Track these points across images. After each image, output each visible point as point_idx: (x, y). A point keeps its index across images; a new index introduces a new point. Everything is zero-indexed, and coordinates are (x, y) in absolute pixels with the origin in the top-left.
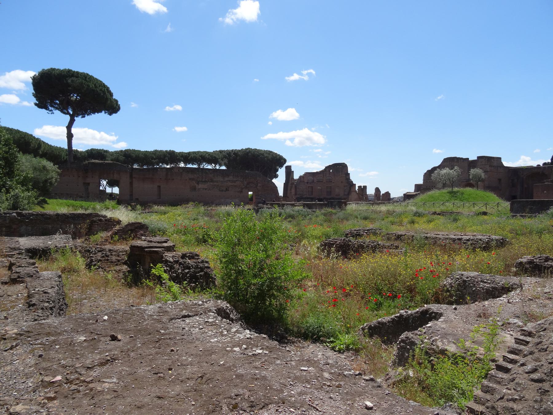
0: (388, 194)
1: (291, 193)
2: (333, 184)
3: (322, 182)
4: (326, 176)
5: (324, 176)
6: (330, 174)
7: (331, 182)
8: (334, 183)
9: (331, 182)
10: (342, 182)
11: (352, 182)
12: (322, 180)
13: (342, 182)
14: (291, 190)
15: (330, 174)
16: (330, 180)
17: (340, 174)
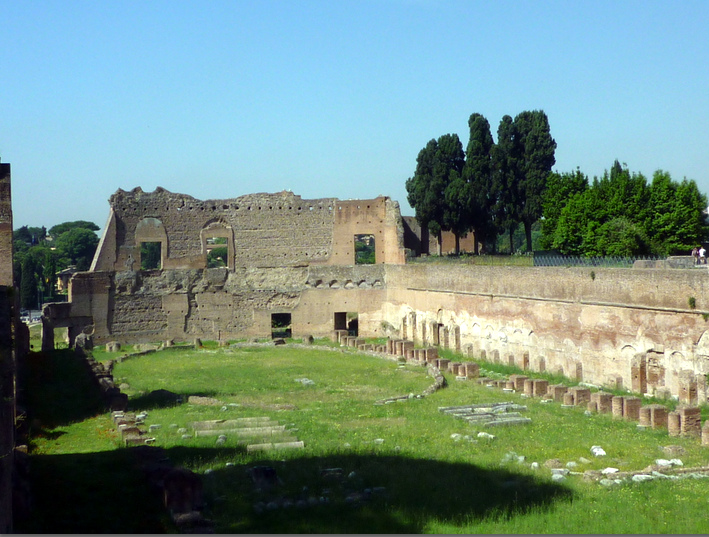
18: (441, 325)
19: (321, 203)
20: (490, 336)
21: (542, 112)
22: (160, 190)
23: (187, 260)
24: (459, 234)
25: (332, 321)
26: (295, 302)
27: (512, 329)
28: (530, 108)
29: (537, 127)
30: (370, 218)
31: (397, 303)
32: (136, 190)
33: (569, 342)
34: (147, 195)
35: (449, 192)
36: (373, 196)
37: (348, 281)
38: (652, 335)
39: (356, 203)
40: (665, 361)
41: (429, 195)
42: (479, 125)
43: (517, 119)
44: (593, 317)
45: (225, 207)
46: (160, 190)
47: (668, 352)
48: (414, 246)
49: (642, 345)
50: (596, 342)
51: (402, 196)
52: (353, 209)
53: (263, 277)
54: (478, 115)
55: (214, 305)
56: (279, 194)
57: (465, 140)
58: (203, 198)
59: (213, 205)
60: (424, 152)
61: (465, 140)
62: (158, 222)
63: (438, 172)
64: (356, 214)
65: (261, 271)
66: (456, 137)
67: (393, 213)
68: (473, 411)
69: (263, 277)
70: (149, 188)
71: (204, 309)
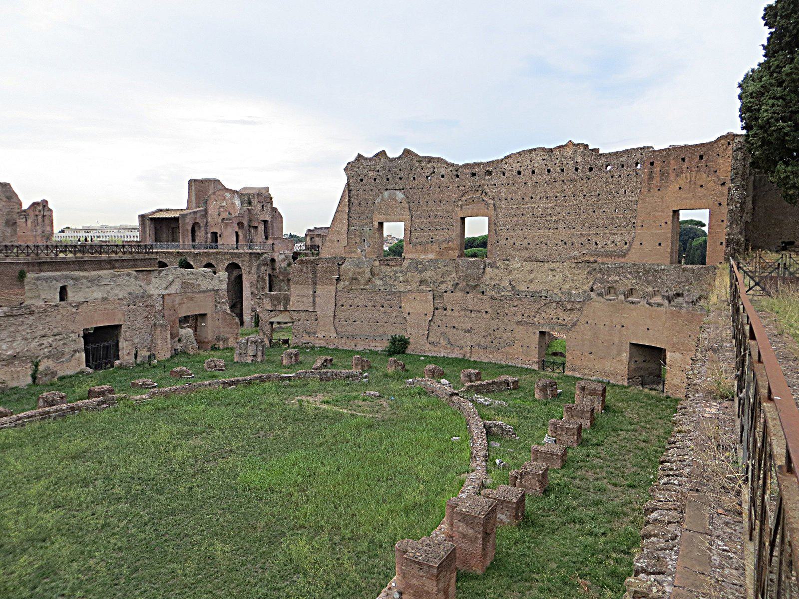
0: (42, 209)
19: (623, 158)
22: (407, 152)
23: (435, 247)
25: (625, 356)
26: (574, 317)
32: (383, 153)
34: (394, 159)
45: (489, 173)
46: (407, 152)
52: (673, 164)
53: (532, 276)
55: (466, 310)
62: (400, 195)
65: (529, 266)
69: (532, 276)
71: (455, 313)
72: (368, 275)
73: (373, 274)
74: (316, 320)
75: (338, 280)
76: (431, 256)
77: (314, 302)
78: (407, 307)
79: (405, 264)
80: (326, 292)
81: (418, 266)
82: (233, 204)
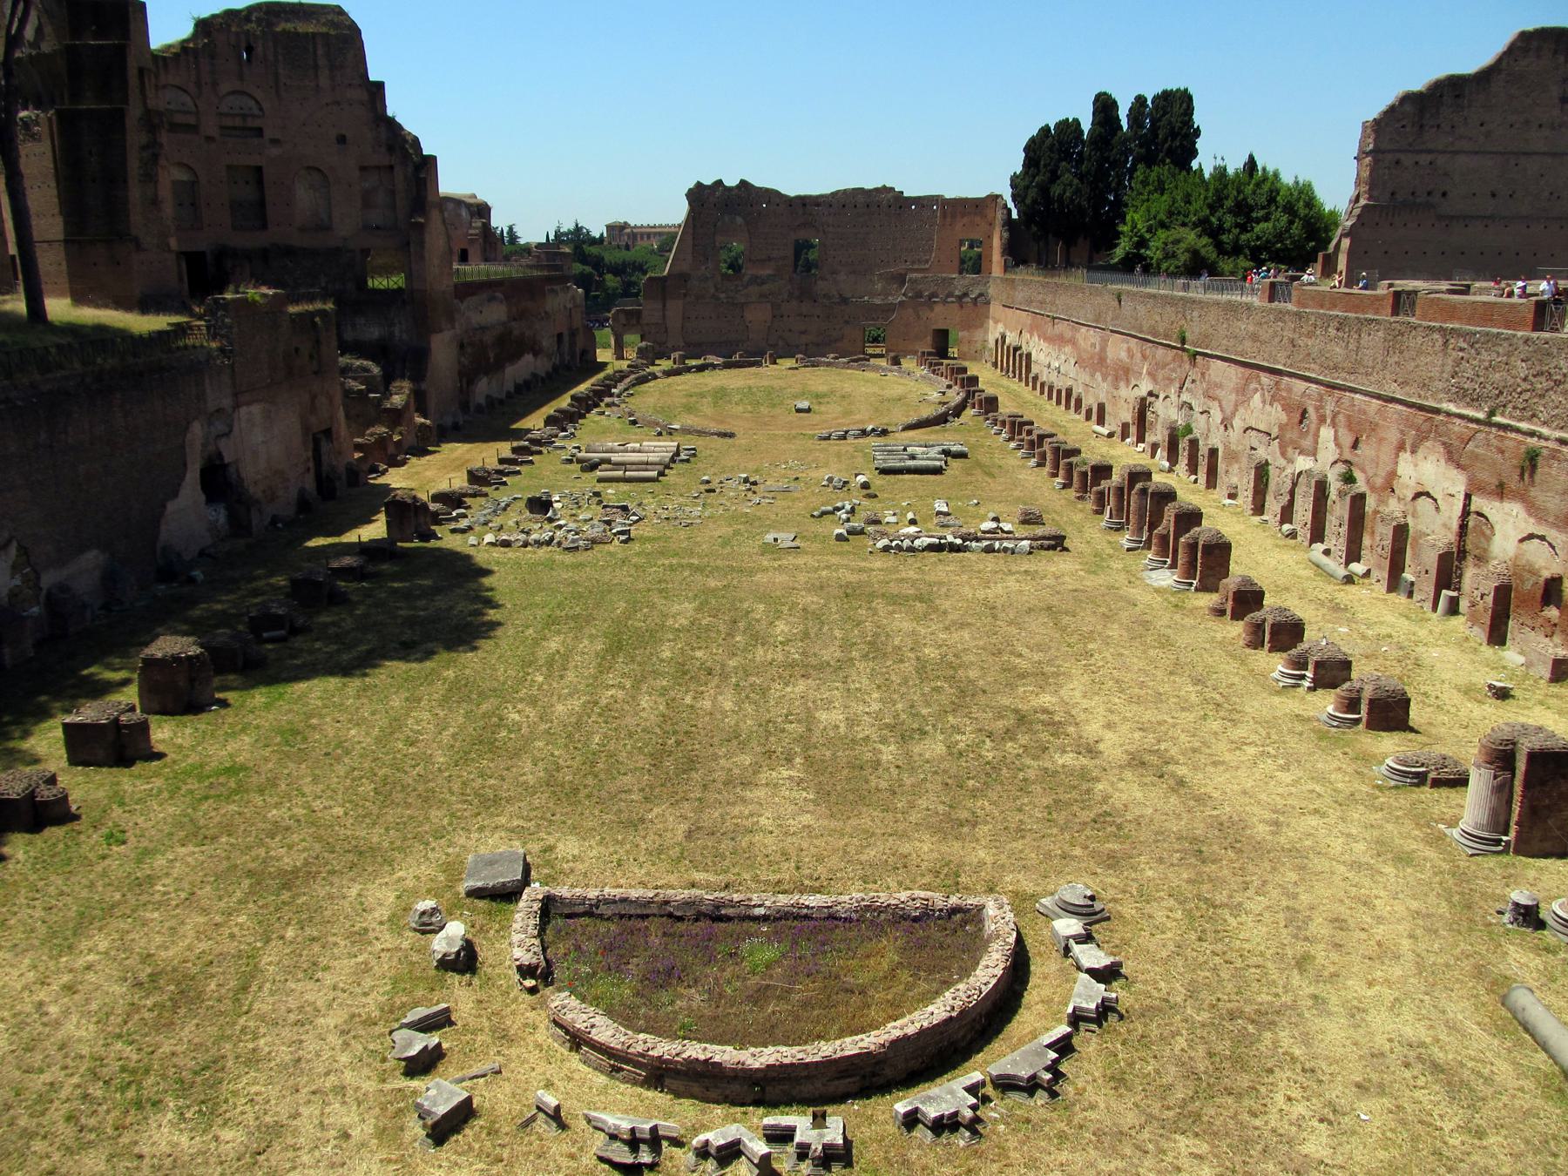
1: (155, 202)
2: (275, 151)
3: (193, 129)
4: (215, 84)
5: (198, 84)
6: (241, 77)
7: (259, 132)
8: (275, 142)
9: (259, 132)
10: (342, 140)
11: (416, 142)
12: (192, 120)
13: (342, 140)
14: (149, 177)
15: (241, 77)
16: (251, 123)
17: (324, 81)
18: (1020, 348)
20: (1049, 366)
21: (1186, 90)
22: (743, 183)
24: (1070, 243)
25: (929, 339)
27: (1063, 357)
28: (1172, 86)
29: (1176, 109)
30: (978, 219)
31: (996, 322)
32: (719, 183)
33: (1098, 376)
34: (730, 189)
35: (1056, 190)
36: (983, 195)
37: (950, 295)
38: (1152, 375)
39: (967, 199)
40: (1158, 406)
41: (1032, 193)
42: (1104, 106)
43: (1155, 99)
44: (1119, 350)
46: (743, 183)
47: (1162, 396)
48: (1017, 254)
49: (1145, 387)
50: (1117, 379)
51: (1007, 194)
54: (1105, 94)
55: (800, 315)
56: (876, 190)
57: (1086, 126)
58: (792, 194)
59: (804, 201)
60: (1032, 140)
61: (1086, 126)
62: (739, 220)
63: (1045, 166)
64: (963, 215)
66: (1077, 122)
67: (1000, 215)
68: (905, 450)
70: (731, 181)
72: (712, 291)
73: (717, 289)
74: (666, 331)
75: (685, 295)
76: (769, 272)
77: (664, 316)
78: (748, 316)
79: (746, 279)
80: (675, 308)
81: (755, 280)
82: (460, 215)
